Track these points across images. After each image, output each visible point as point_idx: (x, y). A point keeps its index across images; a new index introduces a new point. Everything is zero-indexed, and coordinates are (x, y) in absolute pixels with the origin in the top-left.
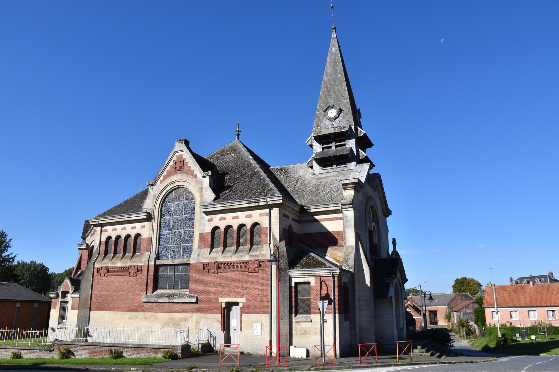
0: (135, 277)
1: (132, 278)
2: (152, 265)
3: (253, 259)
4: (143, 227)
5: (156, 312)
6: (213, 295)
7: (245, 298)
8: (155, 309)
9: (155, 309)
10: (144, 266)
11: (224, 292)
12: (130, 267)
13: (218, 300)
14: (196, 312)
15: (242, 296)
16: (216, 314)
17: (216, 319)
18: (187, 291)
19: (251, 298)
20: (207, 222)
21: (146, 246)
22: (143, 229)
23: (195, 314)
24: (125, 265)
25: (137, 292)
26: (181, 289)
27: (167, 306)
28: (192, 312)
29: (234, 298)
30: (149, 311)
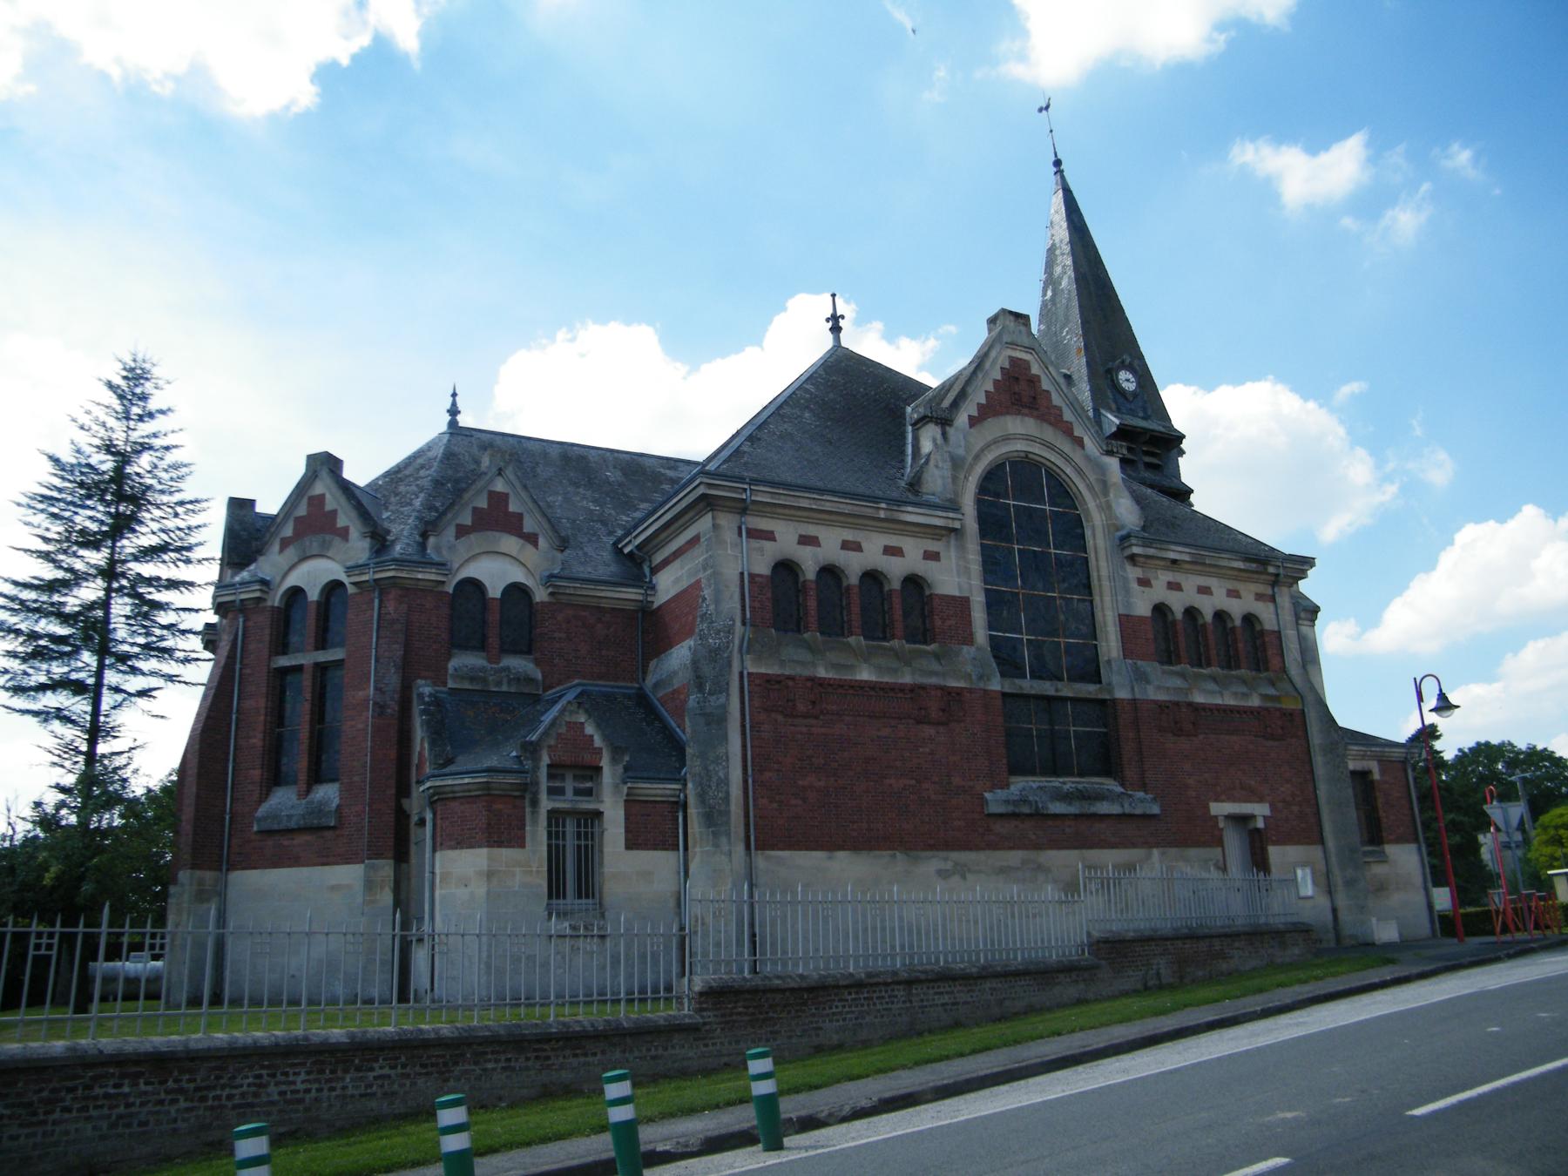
0: (941, 729)
1: (929, 731)
2: (995, 691)
3: (1269, 704)
4: (931, 556)
5: (1038, 847)
6: (1194, 794)
7: (1267, 805)
8: (1033, 837)
9: (1033, 837)
10: (970, 691)
11: (1219, 789)
12: (915, 690)
13: (1207, 808)
14: (1157, 845)
15: (1261, 800)
16: (1208, 849)
17: (1211, 863)
18: (1111, 785)
19: (1280, 805)
20: (1134, 586)
21: (952, 622)
22: (932, 564)
23: (1156, 852)
24: (893, 681)
25: (957, 780)
26: (1081, 775)
27: (1070, 826)
28: (1148, 845)
29: (1243, 805)
30: (1012, 845)
